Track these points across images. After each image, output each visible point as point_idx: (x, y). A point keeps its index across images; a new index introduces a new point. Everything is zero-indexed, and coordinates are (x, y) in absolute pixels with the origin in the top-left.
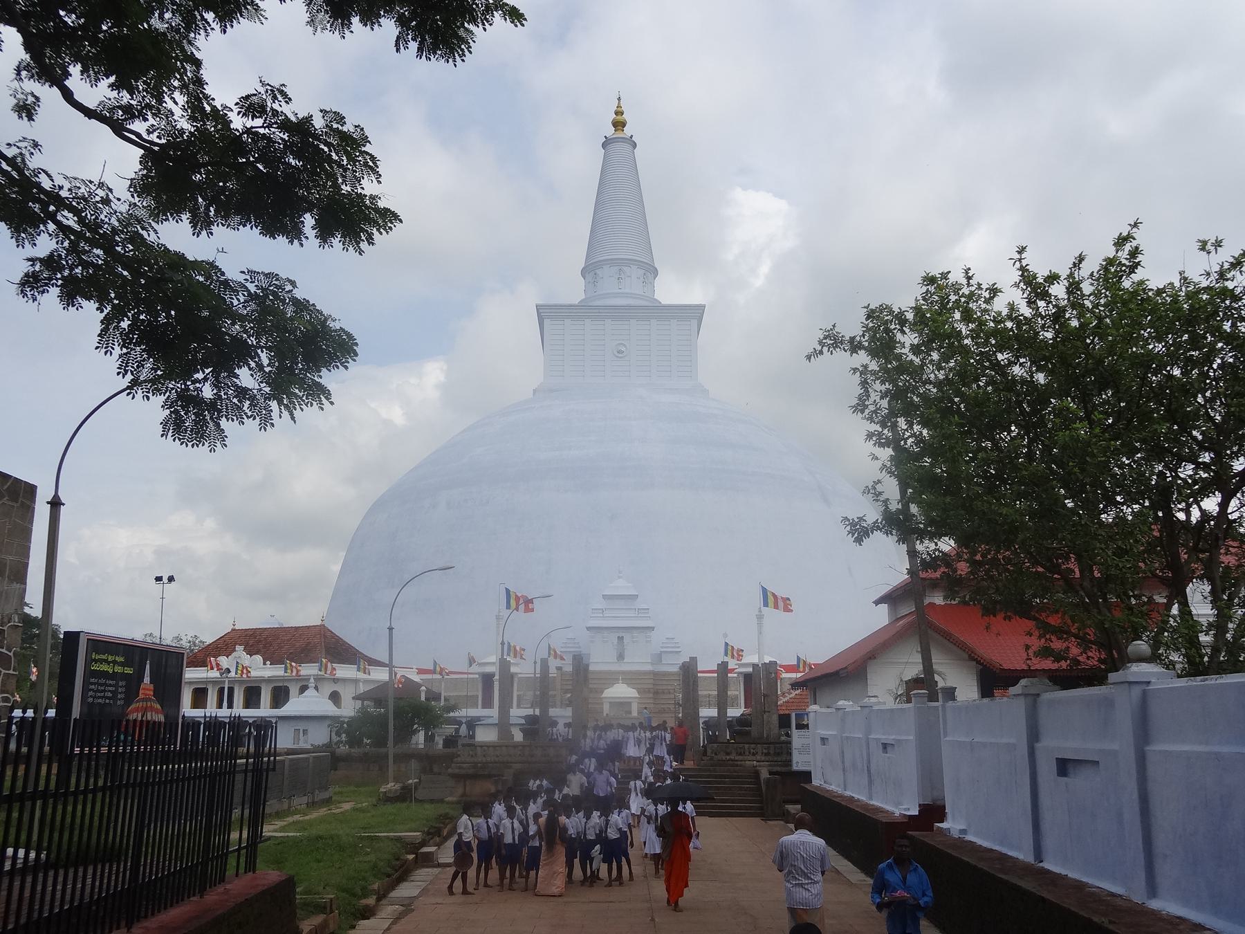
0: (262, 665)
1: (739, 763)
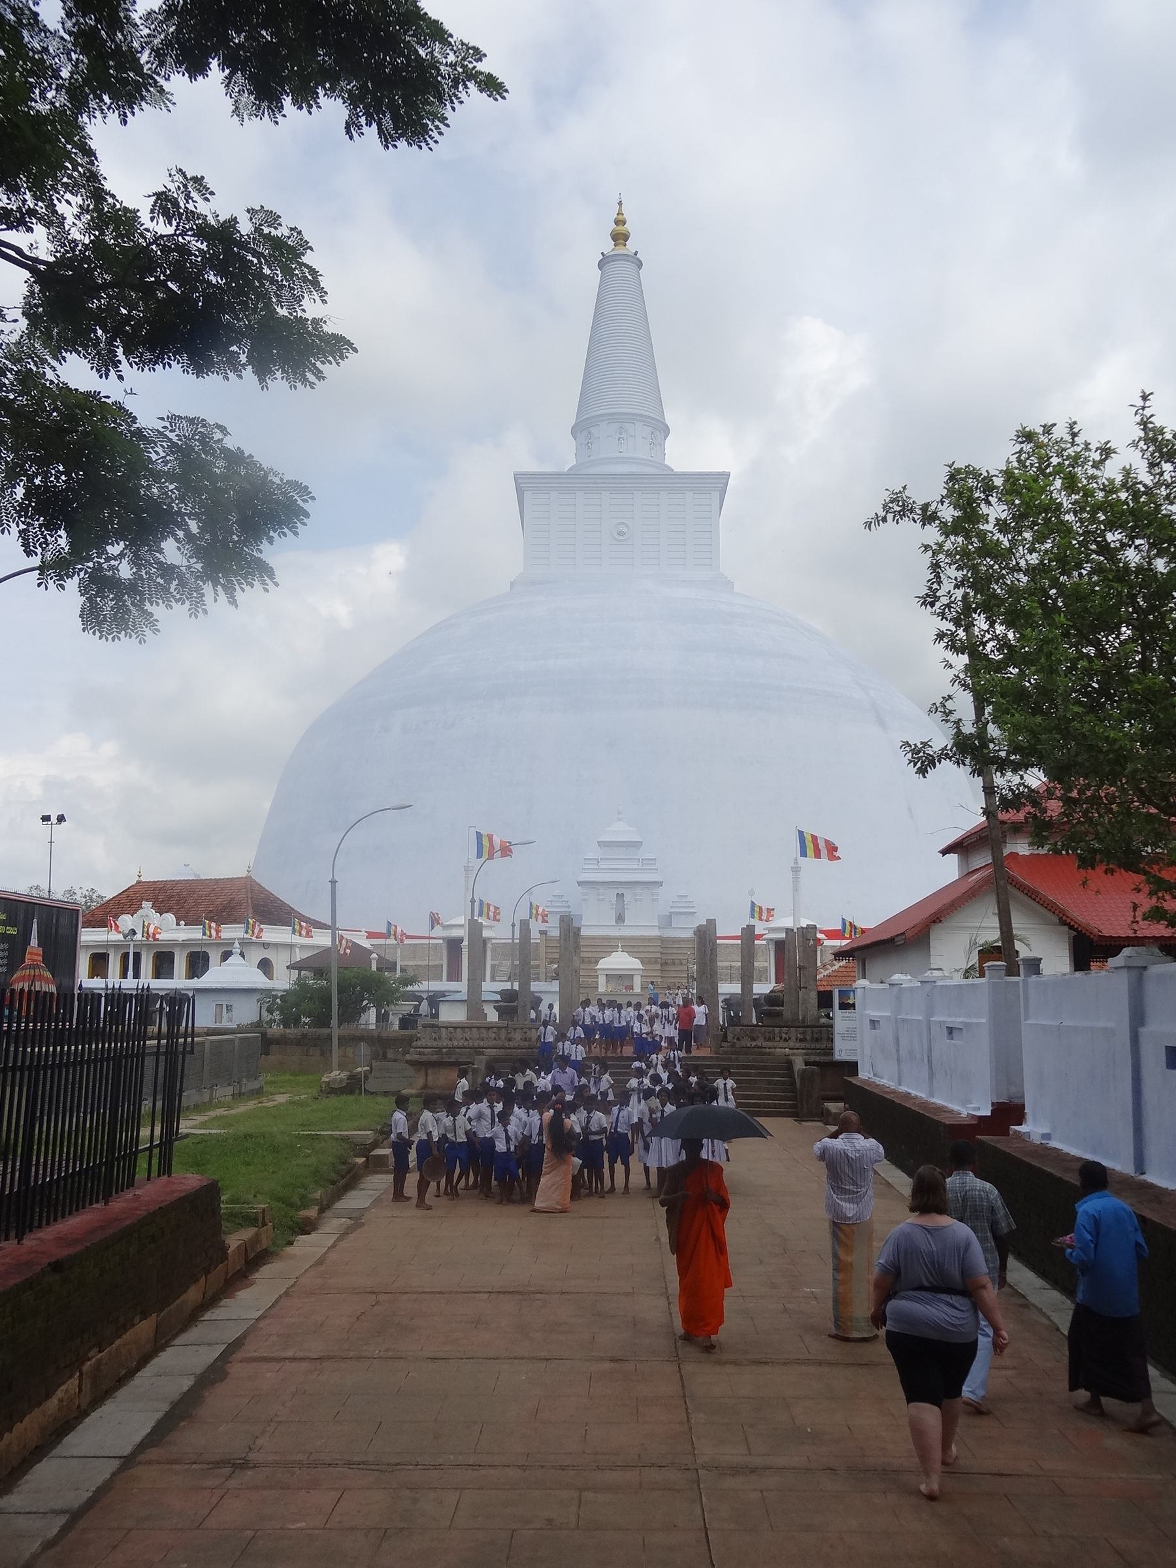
0: (175, 926)
1: (767, 1050)
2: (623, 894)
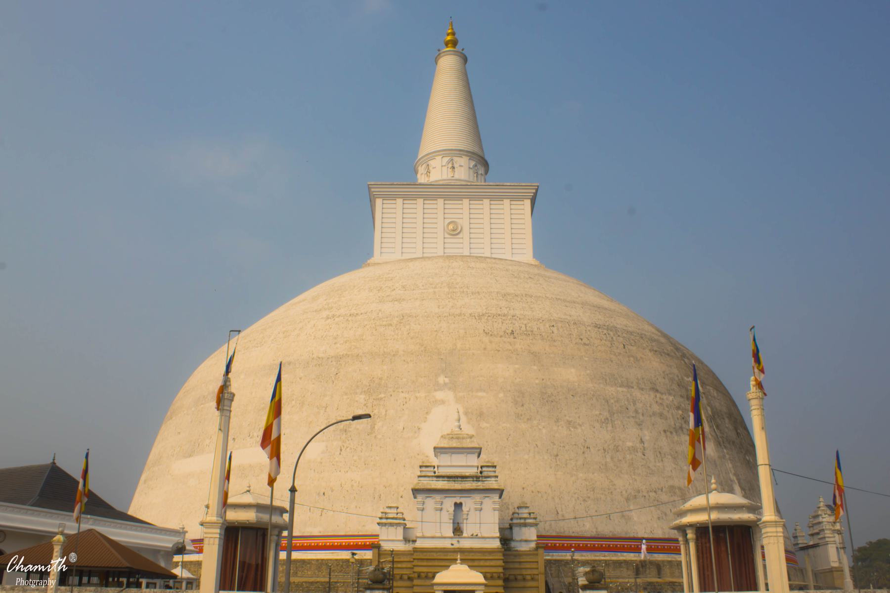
2: (461, 504)
